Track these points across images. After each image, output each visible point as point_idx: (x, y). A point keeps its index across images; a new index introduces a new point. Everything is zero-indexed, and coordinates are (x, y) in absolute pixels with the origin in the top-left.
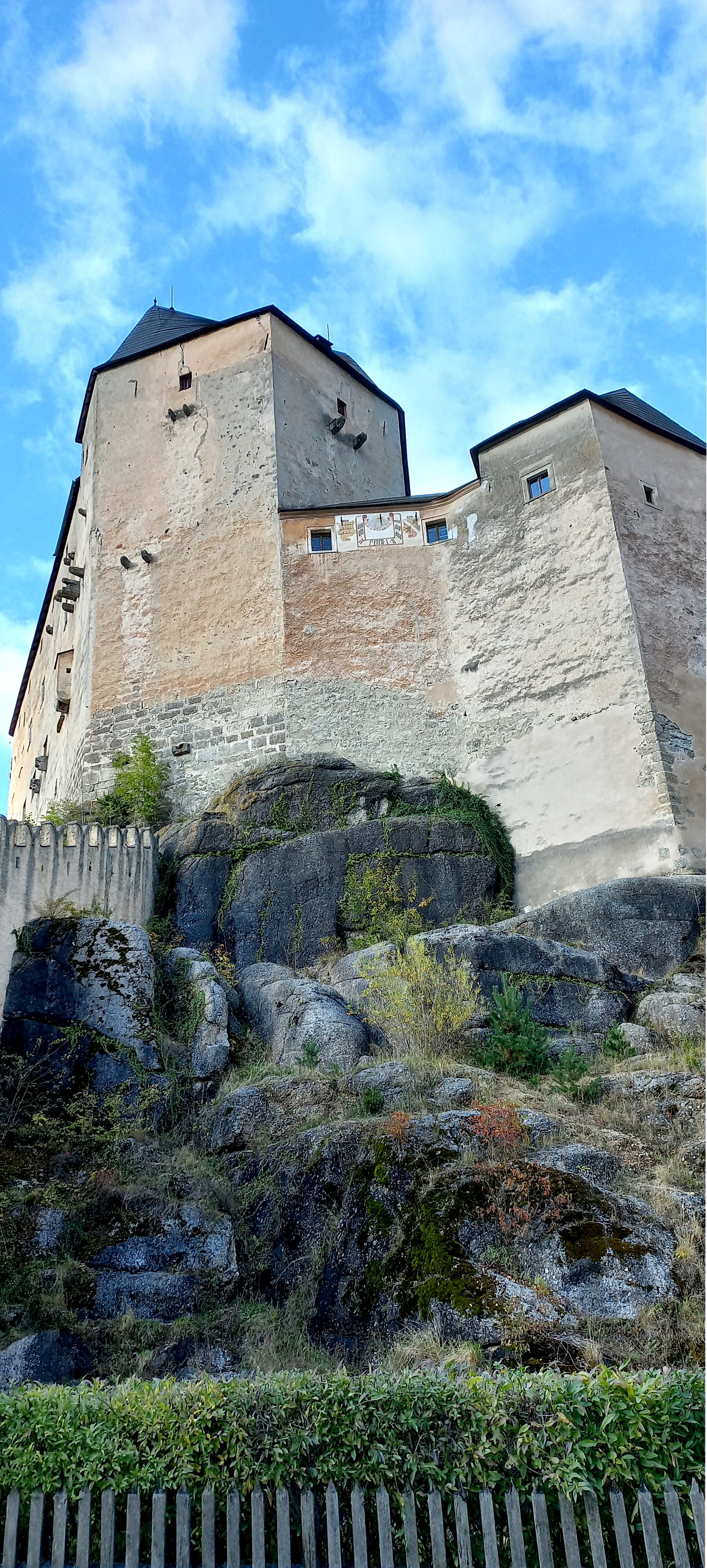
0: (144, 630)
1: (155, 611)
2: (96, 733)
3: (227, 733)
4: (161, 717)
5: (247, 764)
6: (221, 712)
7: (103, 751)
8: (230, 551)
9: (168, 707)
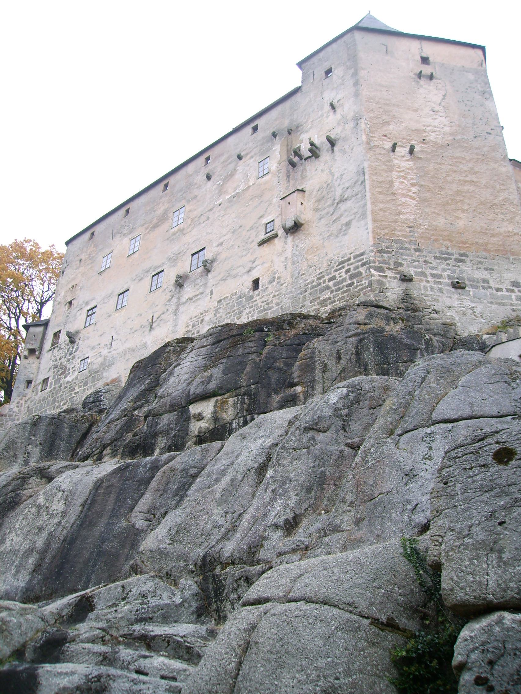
0: (413, 195)
1: (421, 186)
2: (380, 252)
3: (492, 284)
4: (436, 257)
5: (513, 310)
6: (486, 269)
7: (387, 266)
8: (476, 169)
9: (441, 252)
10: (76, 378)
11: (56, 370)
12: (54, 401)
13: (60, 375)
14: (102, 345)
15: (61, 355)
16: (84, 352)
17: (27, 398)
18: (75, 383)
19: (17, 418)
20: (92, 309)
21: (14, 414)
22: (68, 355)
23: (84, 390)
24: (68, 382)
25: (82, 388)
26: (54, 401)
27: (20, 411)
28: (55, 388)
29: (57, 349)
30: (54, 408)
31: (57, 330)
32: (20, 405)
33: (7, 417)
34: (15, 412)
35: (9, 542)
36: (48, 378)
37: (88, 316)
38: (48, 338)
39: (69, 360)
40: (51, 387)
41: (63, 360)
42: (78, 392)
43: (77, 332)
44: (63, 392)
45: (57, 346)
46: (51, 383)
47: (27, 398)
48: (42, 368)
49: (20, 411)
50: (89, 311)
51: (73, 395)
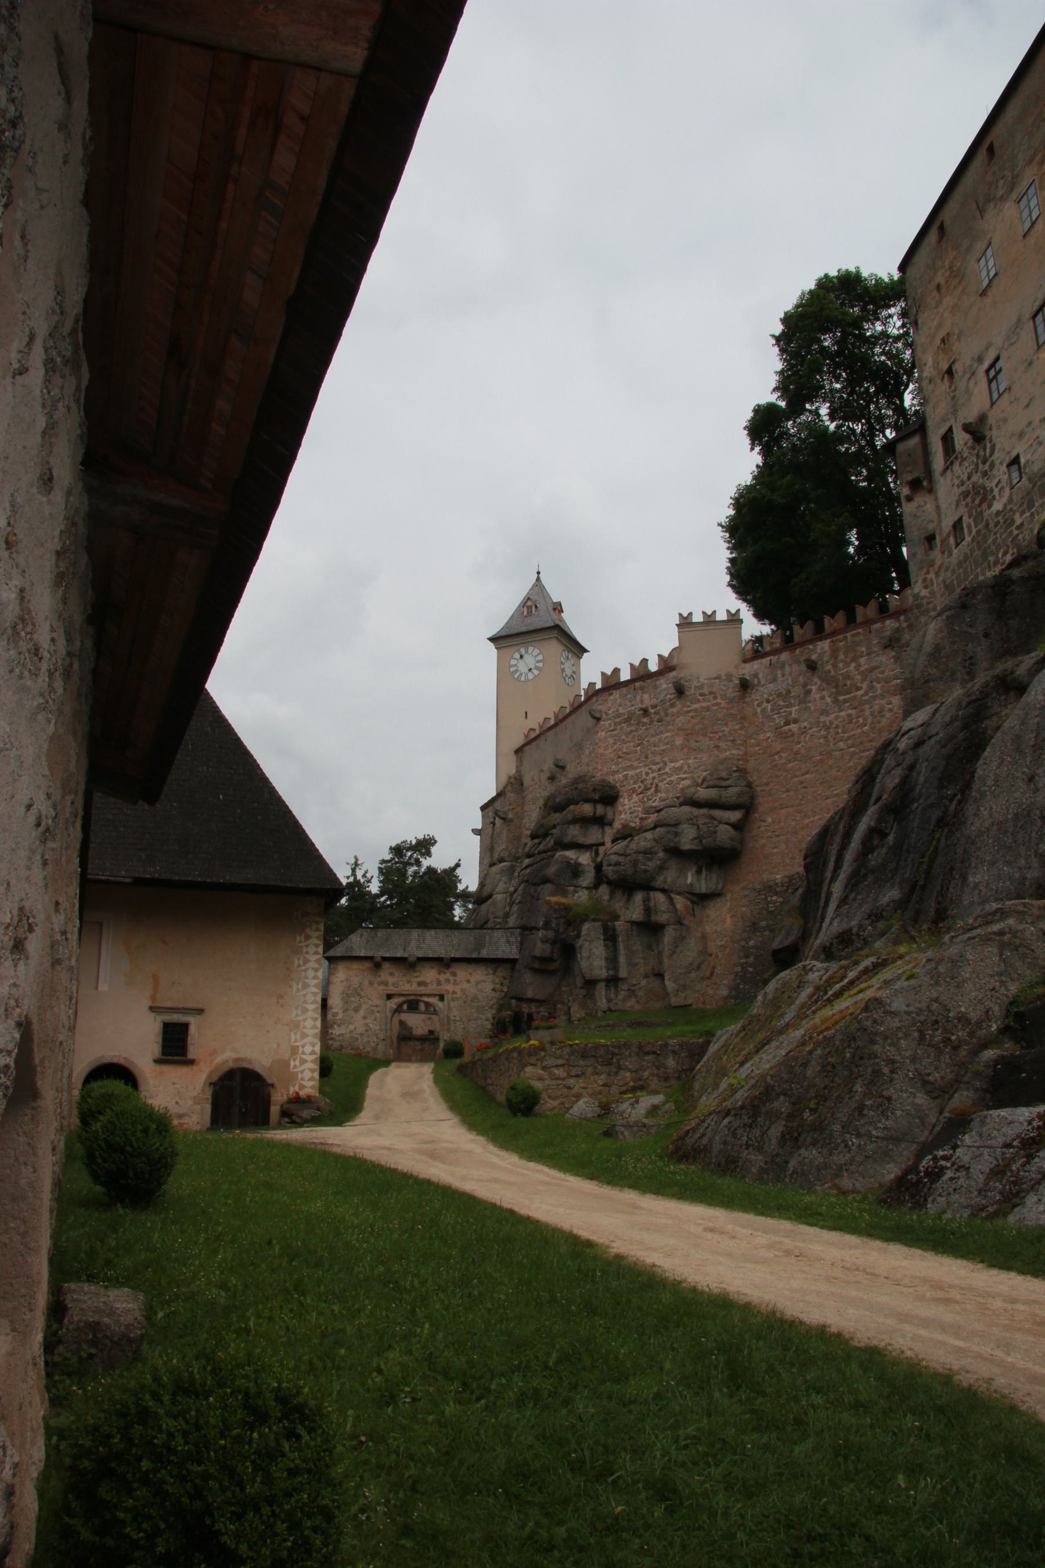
10: (1010, 500)
11: (968, 500)
12: (985, 555)
13: (980, 505)
14: (1036, 422)
15: (969, 470)
16: (1007, 449)
17: (936, 567)
18: (1011, 510)
19: (931, 606)
20: (993, 365)
21: (925, 601)
22: (981, 466)
23: (1032, 516)
24: (998, 513)
25: (1027, 514)
26: (985, 555)
27: (932, 593)
28: (978, 532)
29: (957, 463)
30: (989, 567)
31: (943, 430)
32: (928, 583)
33: (916, 611)
34: (926, 597)
35: (985, 813)
36: (960, 520)
37: (990, 382)
38: (933, 450)
39: (985, 474)
40: (970, 532)
41: (974, 478)
42: (1022, 524)
43: (982, 418)
44: (995, 534)
45: (956, 458)
46: (969, 527)
47: (936, 567)
48: (943, 506)
49: (932, 593)
50: (987, 371)
51: (1016, 532)
